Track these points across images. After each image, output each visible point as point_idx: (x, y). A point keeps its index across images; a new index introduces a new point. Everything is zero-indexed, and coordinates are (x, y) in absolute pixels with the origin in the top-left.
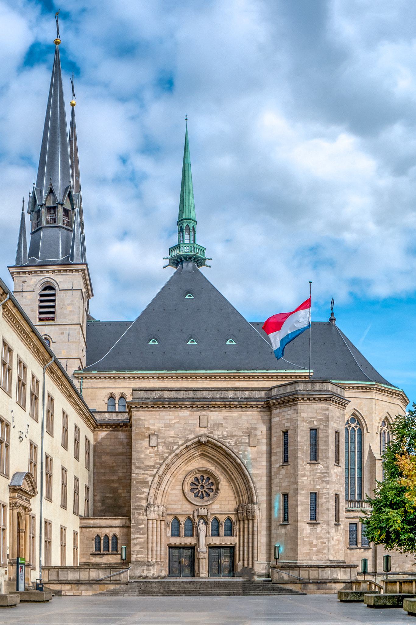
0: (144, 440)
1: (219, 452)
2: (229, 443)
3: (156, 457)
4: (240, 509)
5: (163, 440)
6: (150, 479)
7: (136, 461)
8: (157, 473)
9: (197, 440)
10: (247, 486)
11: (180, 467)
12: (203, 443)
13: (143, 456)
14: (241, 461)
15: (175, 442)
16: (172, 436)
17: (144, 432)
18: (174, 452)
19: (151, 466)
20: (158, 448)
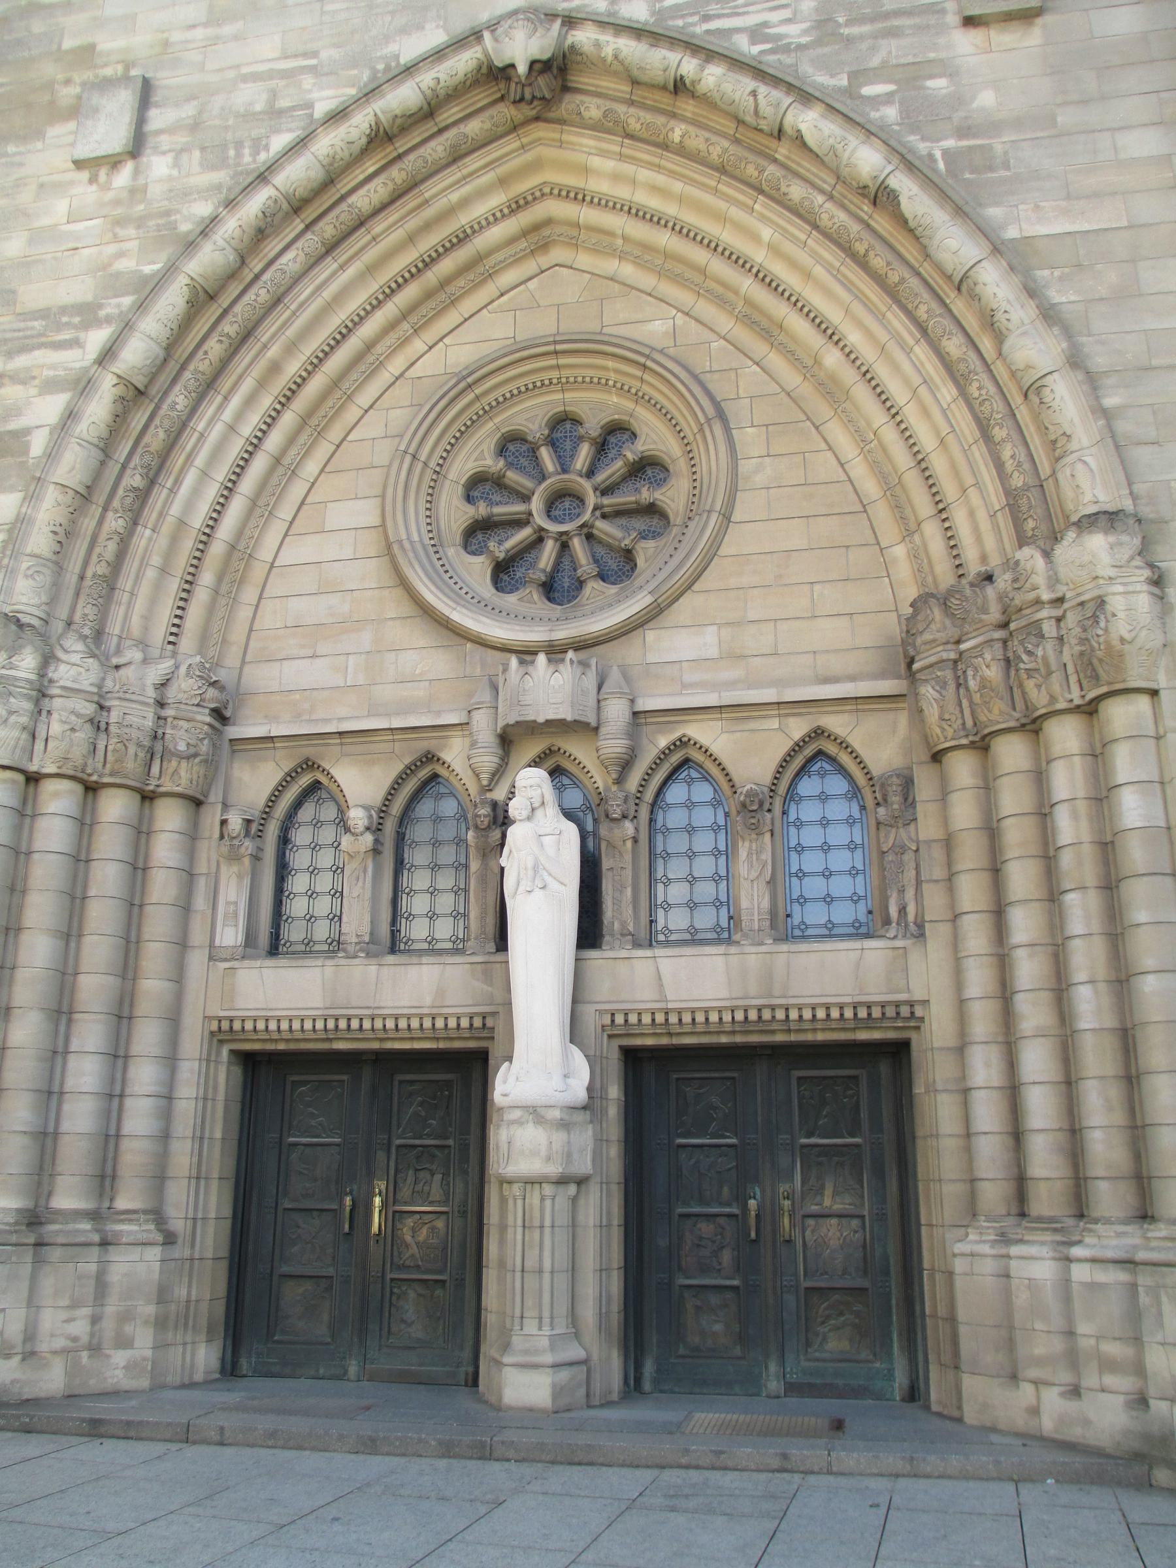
0: (40, 134)
1: (681, 151)
2: (756, 34)
3: (116, 239)
4: (937, 625)
5: (189, 111)
6: (50, 408)
8: (107, 355)
9: (463, 63)
10: (980, 387)
11: (353, 343)
12: (522, 69)
15: (283, 103)
16: (261, 68)
17: (50, 86)
18: (262, 178)
19: (63, 310)
20: (137, 172)
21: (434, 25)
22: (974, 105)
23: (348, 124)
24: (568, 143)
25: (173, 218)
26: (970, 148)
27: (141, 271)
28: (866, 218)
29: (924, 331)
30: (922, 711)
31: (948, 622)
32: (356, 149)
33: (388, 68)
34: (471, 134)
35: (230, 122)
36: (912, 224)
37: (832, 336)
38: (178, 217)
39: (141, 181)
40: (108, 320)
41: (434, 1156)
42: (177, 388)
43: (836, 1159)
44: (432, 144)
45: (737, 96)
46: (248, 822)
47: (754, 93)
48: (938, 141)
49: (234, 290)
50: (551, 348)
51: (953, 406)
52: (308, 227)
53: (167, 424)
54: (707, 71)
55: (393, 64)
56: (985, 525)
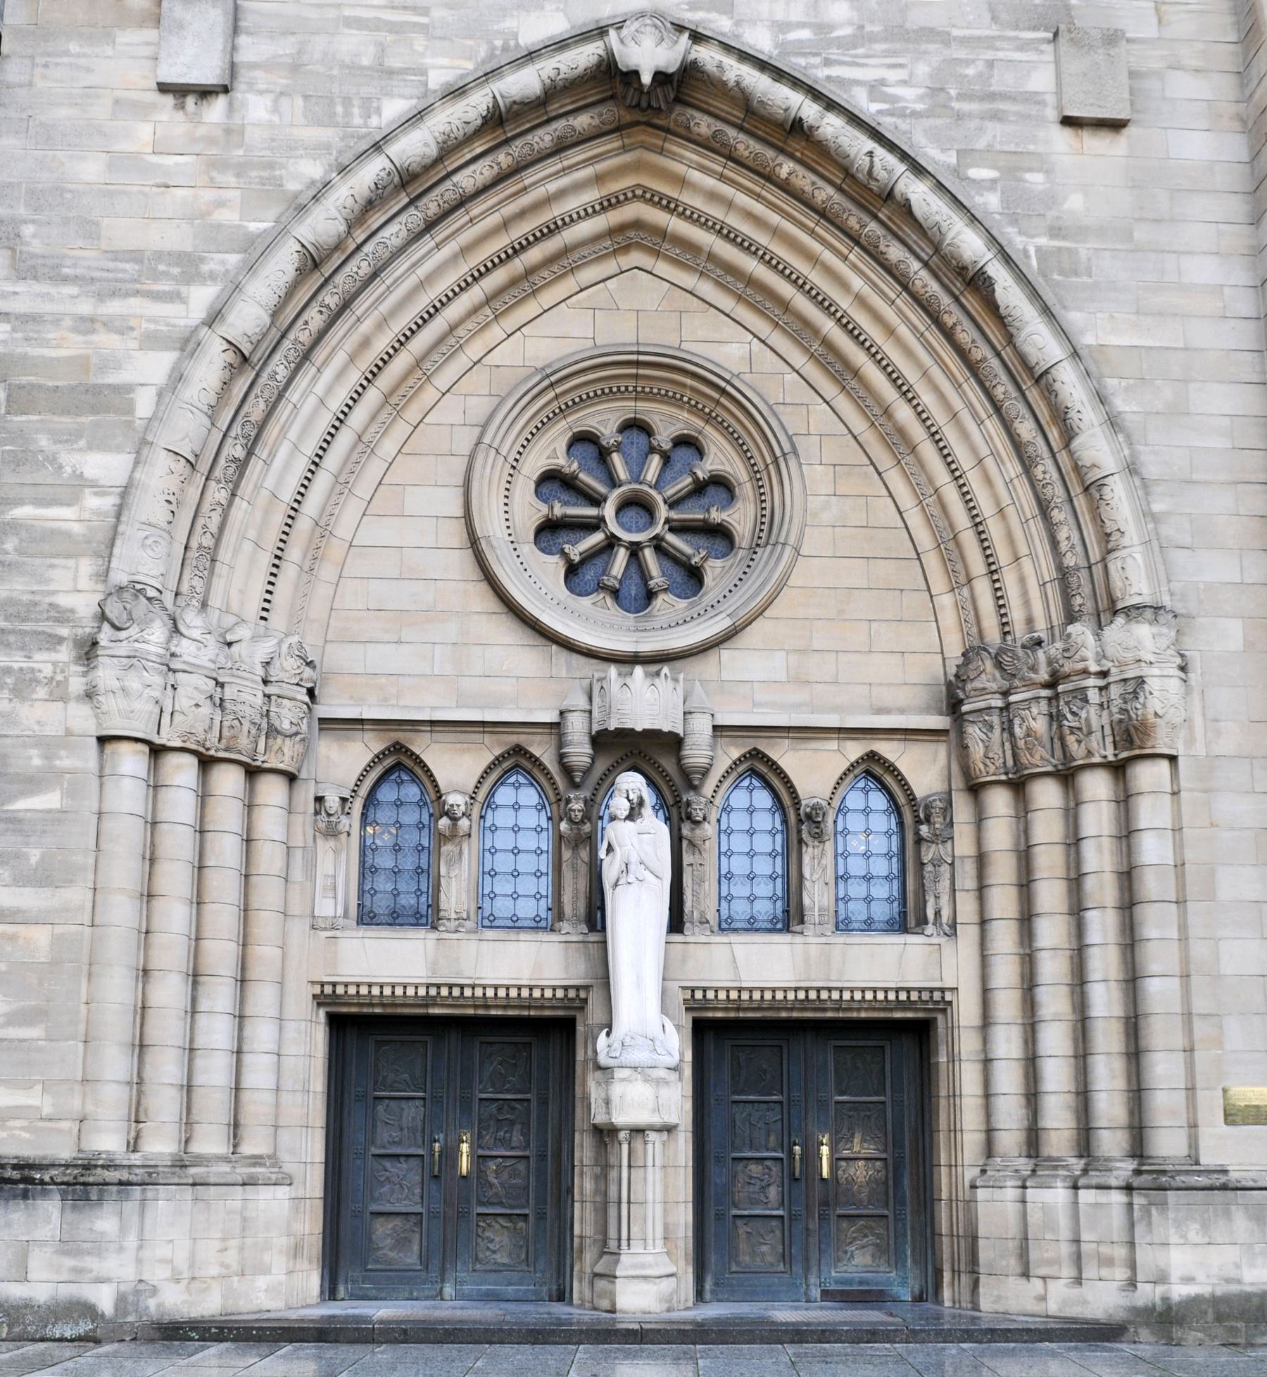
1: (785, 187)
2: (876, 89)
3: (212, 184)
4: (988, 678)
5: (285, 48)
7: (22, 211)
8: (214, 318)
9: (584, 57)
10: (1045, 469)
12: (646, 79)
13: (90, 170)
14: (992, 240)
15: (394, 62)
18: (377, 147)
19: (159, 256)
20: (231, 108)
21: (554, 7)
22: (1066, 206)
23: (465, 102)
24: (669, 152)
25: (278, 173)
26: (1060, 249)
27: (246, 228)
28: (957, 293)
29: (997, 408)
30: (967, 747)
31: (998, 675)
32: (470, 129)
33: (505, 48)
34: (579, 128)
35: (335, 72)
36: (1003, 311)
37: (906, 393)
38: (283, 172)
39: (237, 120)
40: (212, 276)
41: (513, 1108)
42: (278, 356)
43: (862, 1114)
44: (540, 132)
45: (852, 152)
46: (344, 800)
47: (870, 154)
48: (1033, 237)
49: (337, 259)
50: (634, 357)
51: (1016, 481)
52: (412, 202)
53: (267, 393)
54: (826, 120)
55: (512, 43)
56: (1034, 593)
